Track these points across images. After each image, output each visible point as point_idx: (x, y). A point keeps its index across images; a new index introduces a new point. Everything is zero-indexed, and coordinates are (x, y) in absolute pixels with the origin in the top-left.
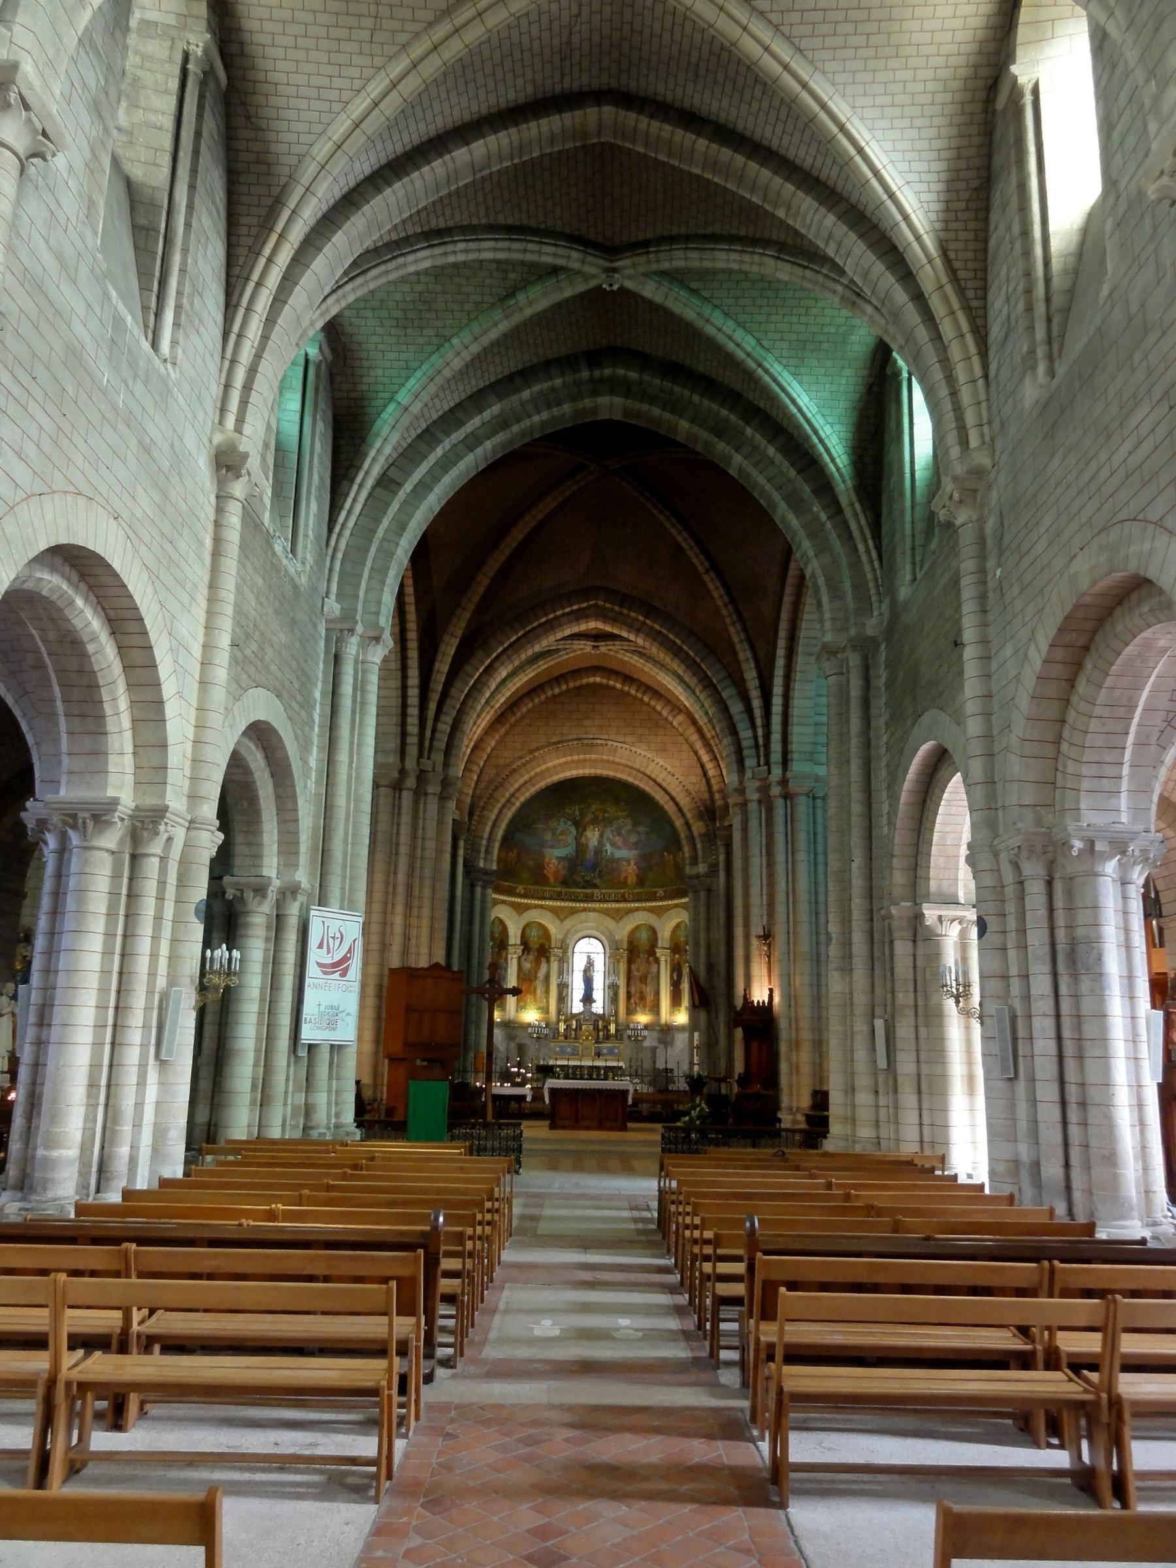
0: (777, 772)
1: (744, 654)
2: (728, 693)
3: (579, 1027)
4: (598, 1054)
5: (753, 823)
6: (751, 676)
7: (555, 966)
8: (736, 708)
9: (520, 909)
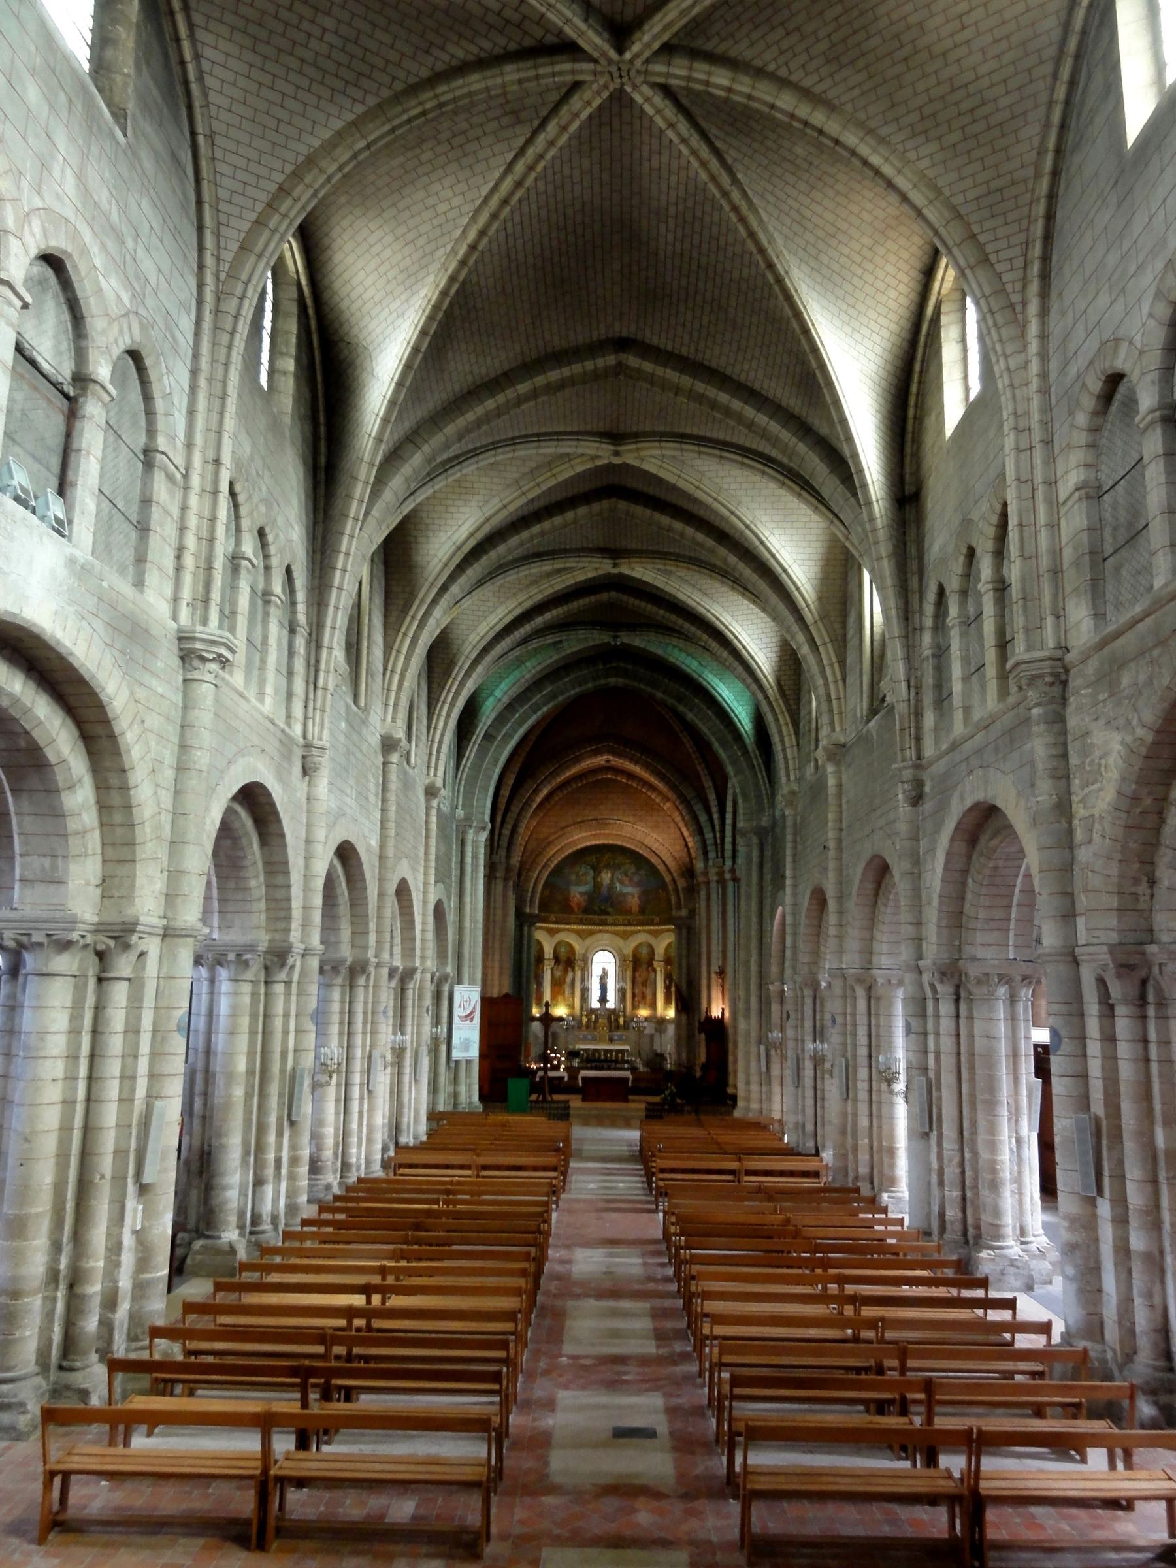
0: (728, 863)
1: (708, 784)
2: (698, 807)
3: (596, 1021)
4: (611, 1040)
5: (714, 897)
6: (712, 798)
7: (578, 973)
8: (703, 818)
9: (552, 932)
